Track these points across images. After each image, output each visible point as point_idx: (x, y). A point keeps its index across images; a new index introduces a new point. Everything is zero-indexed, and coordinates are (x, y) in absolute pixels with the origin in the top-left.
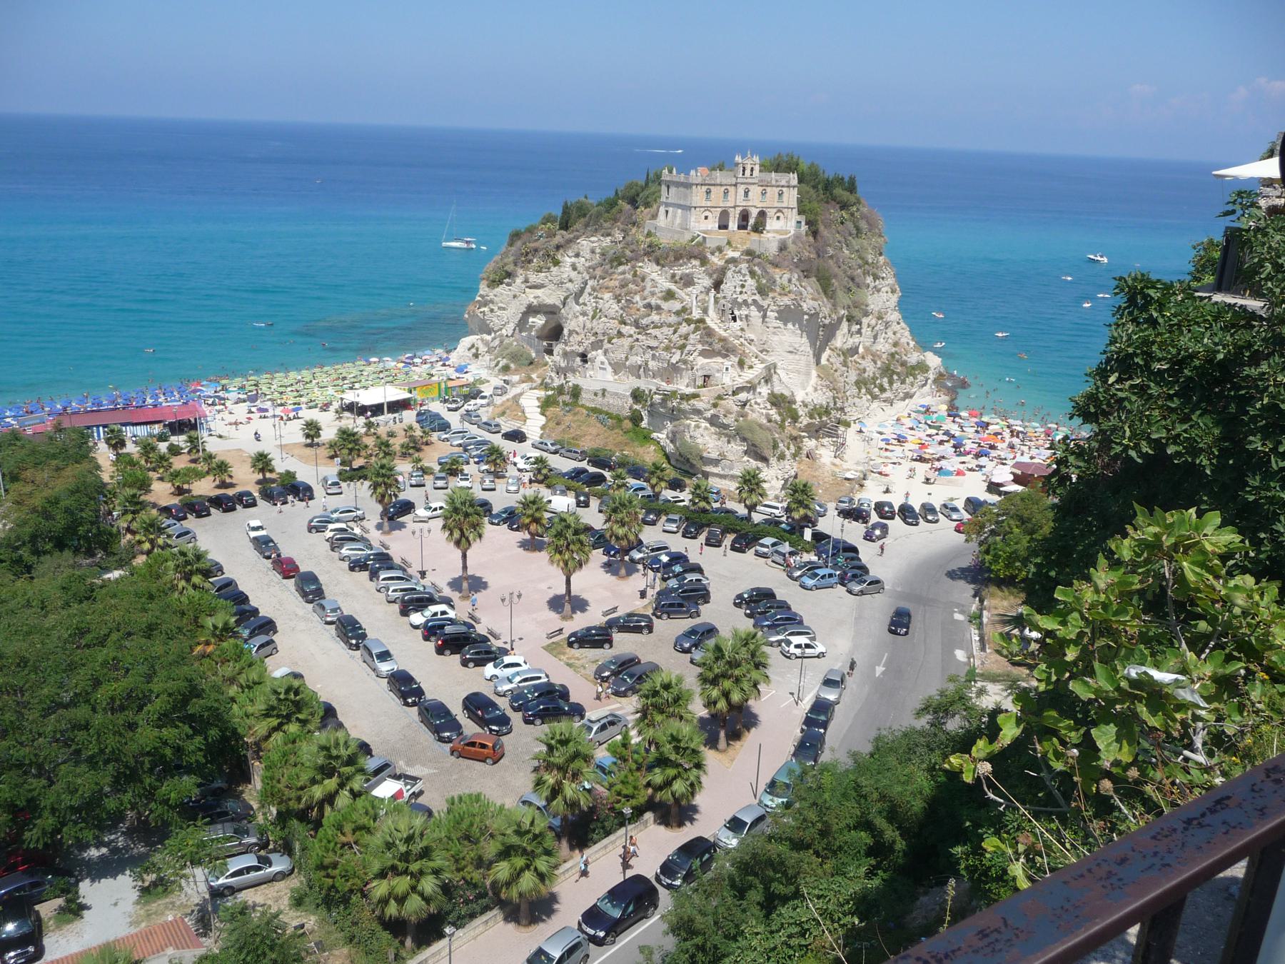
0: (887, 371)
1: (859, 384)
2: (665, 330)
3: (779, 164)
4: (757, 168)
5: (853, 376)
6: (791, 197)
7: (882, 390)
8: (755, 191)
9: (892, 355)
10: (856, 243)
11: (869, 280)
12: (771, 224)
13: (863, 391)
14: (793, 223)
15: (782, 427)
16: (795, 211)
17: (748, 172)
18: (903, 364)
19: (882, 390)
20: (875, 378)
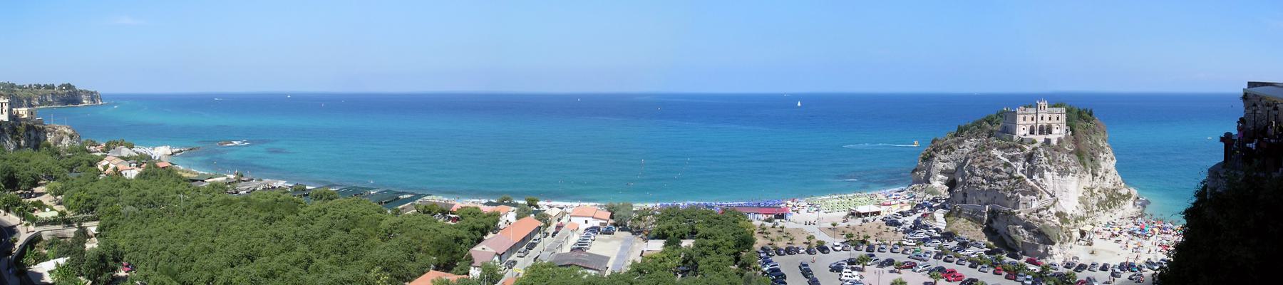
1: (1098, 205)
3: (1055, 102)
4: (1047, 106)
5: (1096, 202)
6: (1063, 118)
7: (1110, 207)
8: (1046, 117)
9: (1114, 190)
10: (1094, 137)
11: (1101, 155)
12: (1055, 131)
13: (1101, 208)
14: (1064, 130)
15: (1061, 228)
16: (1065, 125)
17: (1043, 107)
18: (1120, 194)
19: (1110, 207)
20: (1106, 202)
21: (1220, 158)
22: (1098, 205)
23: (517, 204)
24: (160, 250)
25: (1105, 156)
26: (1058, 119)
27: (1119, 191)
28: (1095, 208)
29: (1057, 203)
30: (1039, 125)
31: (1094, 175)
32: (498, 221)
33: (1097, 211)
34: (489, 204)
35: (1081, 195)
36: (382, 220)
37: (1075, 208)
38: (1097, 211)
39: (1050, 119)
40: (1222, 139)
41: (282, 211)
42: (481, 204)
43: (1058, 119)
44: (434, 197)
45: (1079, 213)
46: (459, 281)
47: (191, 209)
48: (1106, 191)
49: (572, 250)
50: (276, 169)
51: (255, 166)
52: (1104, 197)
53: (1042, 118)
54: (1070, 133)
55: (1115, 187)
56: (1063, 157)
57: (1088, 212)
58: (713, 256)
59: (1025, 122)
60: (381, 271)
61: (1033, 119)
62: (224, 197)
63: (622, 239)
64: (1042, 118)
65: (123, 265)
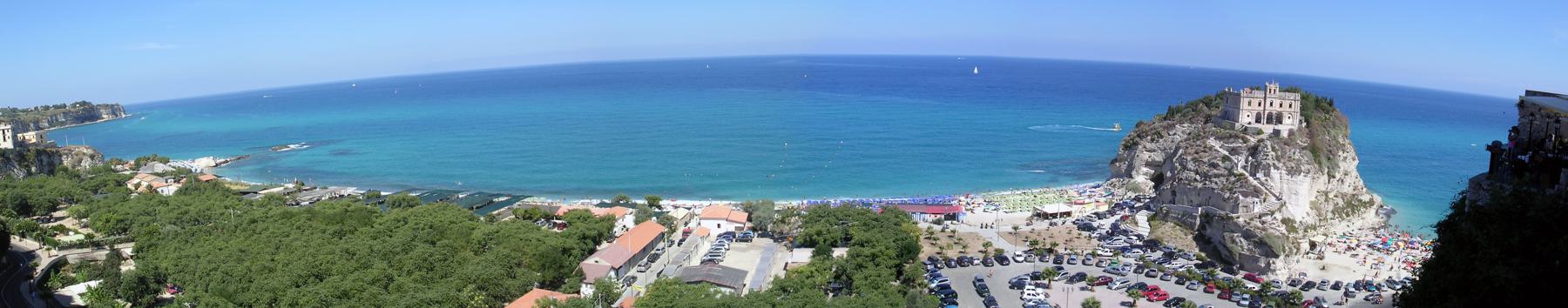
0: (1349, 204)
1: (1333, 212)
2: (1222, 178)
3: (1289, 86)
4: (1278, 90)
5: (1331, 208)
6: (1297, 106)
8: (1277, 103)
9: (1354, 195)
10: (1333, 132)
11: (1340, 153)
12: (1286, 121)
15: (1288, 237)
16: (1299, 114)
17: (1272, 92)
18: (1361, 201)
20: (1343, 209)
21: (1484, 167)
22: (1333, 212)
23: (636, 204)
24: (210, 271)
25: (1345, 155)
26: (1290, 106)
27: (1360, 197)
28: (1330, 215)
29: (1284, 207)
30: (1267, 112)
31: (1331, 176)
32: (613, 226)
33: (1331, 219)
34: (602, 205)
35: (1313, 199)
36: (473, 229)
37: (1305, 215)
38: (1331, 219)
39: (1281, 105)
40: (1489, 148)
41: (354, 222)
42: (592, 206)
43: (1290, 106)
44: (536, 199)
45: (1310, 221)
46: (568, 300)
47: (244, 225)
48: (1343, 196)
49: (702, 263)
50: (343, 174)
51: (318, 172)
52: (1341, 203)
53: (1271, 104)
54: (1304, 124)
55: (1354, 193)
56: (1294, 153)
57: (1320, 220)
58: (871, 270)
59: (1250, 108)
60: (475, 290)
61: (1260, 105)
62: (282, 210)
63: (763, 247)
64: (1271, 104)
65: (167, 287)
